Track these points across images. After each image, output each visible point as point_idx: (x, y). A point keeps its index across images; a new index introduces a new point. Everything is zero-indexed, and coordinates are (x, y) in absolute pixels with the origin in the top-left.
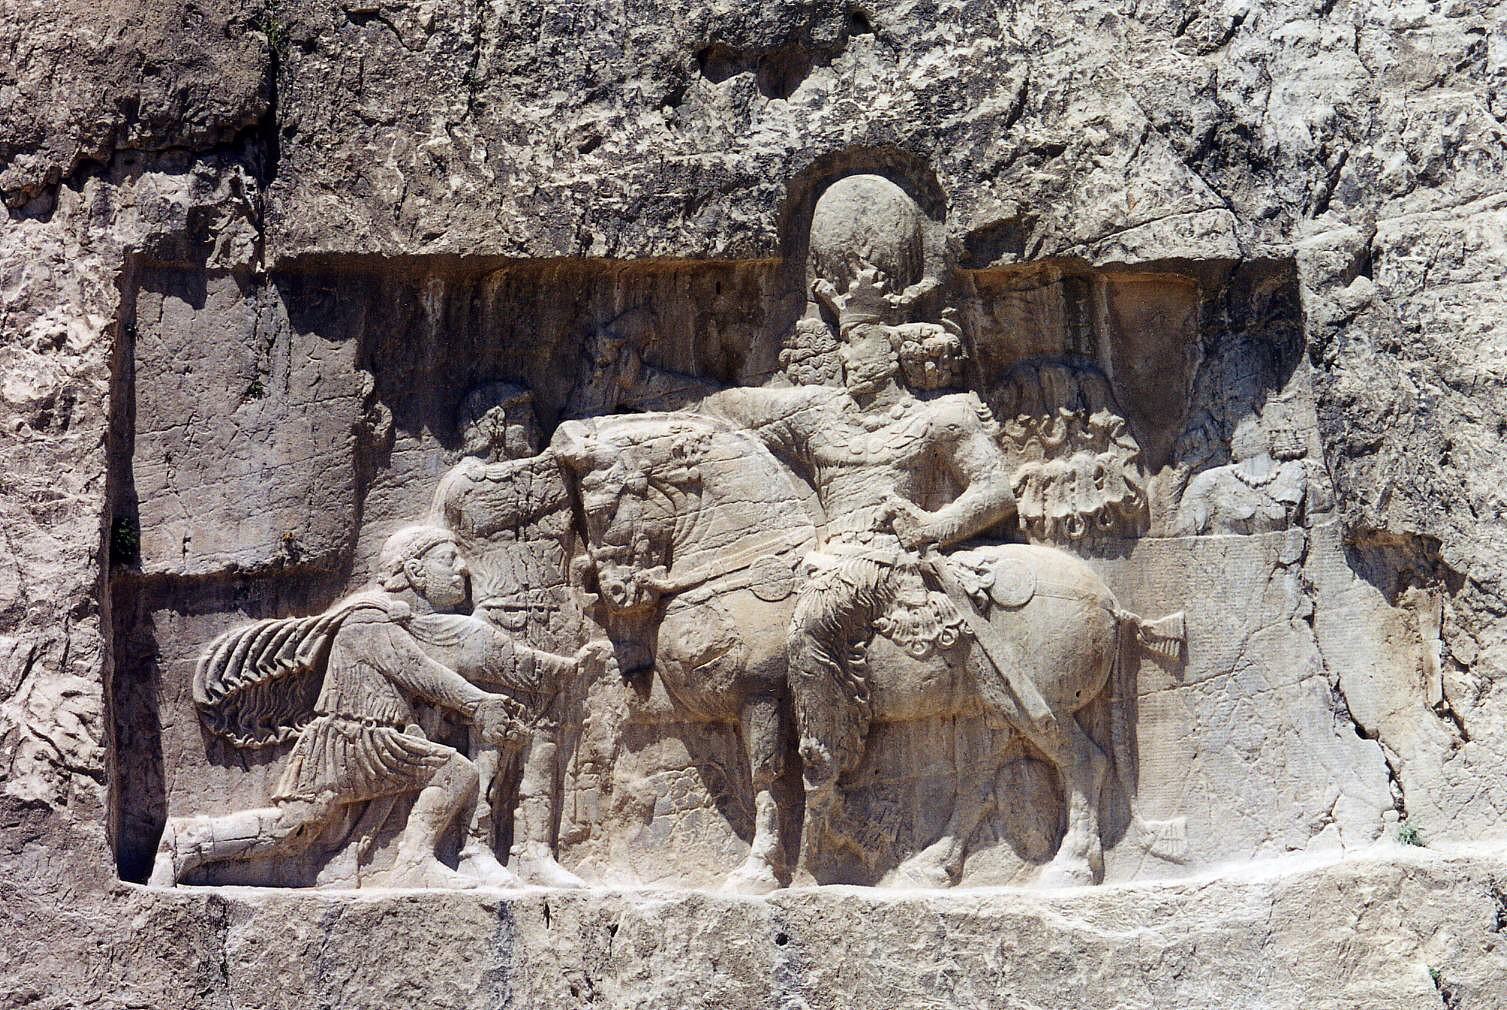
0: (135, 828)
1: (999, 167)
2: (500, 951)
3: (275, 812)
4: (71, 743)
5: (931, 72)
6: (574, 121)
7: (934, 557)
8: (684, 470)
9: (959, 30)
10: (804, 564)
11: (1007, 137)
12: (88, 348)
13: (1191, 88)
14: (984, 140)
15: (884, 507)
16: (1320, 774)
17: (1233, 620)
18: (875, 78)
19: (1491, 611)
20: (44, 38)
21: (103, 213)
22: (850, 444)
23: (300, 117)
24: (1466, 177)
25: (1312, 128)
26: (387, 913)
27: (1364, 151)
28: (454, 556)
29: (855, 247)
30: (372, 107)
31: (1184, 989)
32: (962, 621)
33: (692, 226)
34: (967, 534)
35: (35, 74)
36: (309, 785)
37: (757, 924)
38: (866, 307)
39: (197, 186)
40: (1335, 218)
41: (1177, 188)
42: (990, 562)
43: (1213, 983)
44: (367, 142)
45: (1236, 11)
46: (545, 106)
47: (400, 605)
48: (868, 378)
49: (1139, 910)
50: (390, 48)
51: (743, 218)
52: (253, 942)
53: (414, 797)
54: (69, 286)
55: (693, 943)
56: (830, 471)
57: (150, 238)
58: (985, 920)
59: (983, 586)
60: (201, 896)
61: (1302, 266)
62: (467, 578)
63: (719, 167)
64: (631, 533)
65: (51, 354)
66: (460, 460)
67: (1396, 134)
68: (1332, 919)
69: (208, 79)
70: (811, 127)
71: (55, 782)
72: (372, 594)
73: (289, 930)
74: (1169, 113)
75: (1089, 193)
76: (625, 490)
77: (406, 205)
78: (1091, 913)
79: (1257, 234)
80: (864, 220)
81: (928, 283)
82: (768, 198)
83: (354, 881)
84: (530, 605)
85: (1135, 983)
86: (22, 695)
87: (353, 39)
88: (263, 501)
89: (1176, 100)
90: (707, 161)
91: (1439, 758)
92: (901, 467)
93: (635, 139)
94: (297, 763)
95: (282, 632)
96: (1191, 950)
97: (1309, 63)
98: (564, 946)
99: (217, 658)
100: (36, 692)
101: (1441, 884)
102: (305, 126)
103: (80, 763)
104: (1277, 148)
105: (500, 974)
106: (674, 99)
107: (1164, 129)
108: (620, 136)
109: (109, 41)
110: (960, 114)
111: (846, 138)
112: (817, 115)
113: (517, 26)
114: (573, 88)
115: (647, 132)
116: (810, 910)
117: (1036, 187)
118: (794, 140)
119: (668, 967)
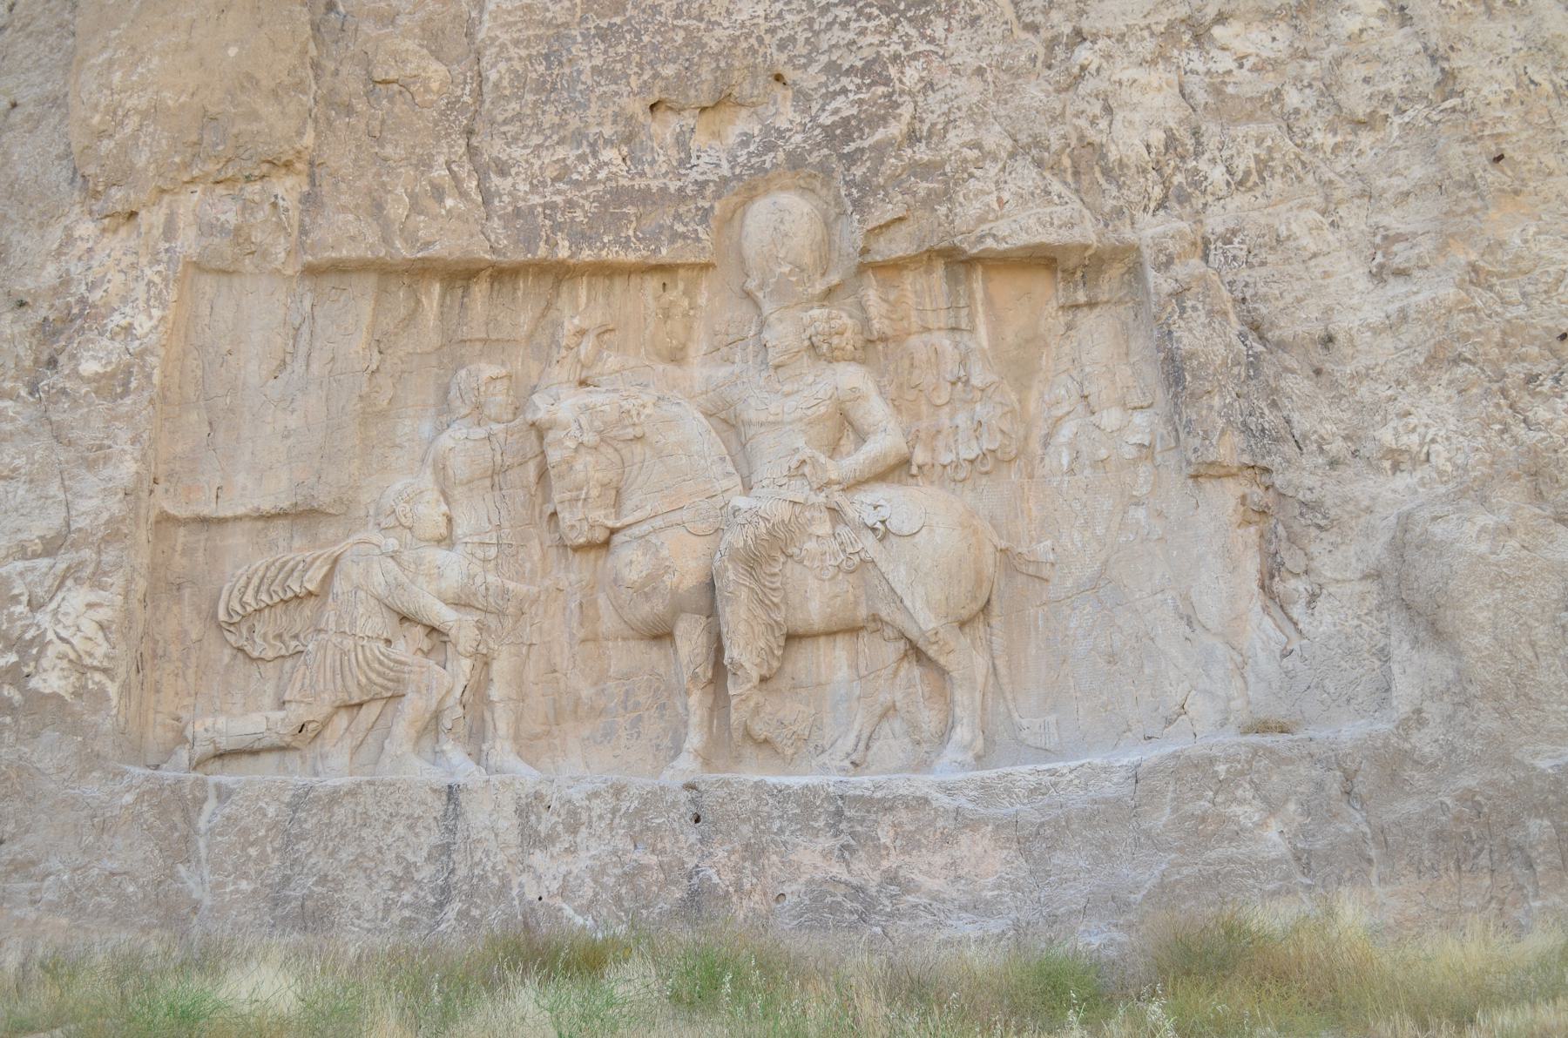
1: (896, 179)
2: (447, 828)
3: (281, 714)
4: (89, 646)
5: (836, 111)
7: (838, 497)
8: (630, 430)
9: (859, 81)
12: (147, 335)
15: (798, 457)
19: (1319, 527)
20: (136, 102)
21: (170, 231)
24: (1276, 184)
25: (1148, 147)
26: (347, 794)
27: (1191, 164)
30: (389, 150)
31: (1058, 858)
35: (128, 130)
39: (244, 208)
45: (1081, 60)
46: (525, 147)
47: (392, 543)
50: (405, 107)
51: (685, 229)
52: (228, 818)
53: (398, 696)
54: (141, 287)
55: (617, 820)
56: (751, 431)
58: (879, 800)
61: (1143, 248)
62: (450, 520)
63: (664, 190)
66: (448, 426)
67: (1216, 153)
68: (1190, 795)
69: (255, 127)
70: (739, 160)
71: (72, 679)
73: (261, 808)
75: (964, 195)
79: (1106, 225)
81: (834, 279)
85: (1012, 853)
86: (53, 605)
90: (655, 185)
91: (1278, 655)
93: (594, 171)
95: (292, 563)
98: (503, 824)
99: (238, 586)
100: (65, 603)
101: (1290, 761)
103: (96, 663)
104: (1121, 160)
105: (446, 849)
109: (182, 100)
110: (859, 141)
111: (768, 165)
114: (548, 132)
115: (606, 164)
116: (722, 793)
117: (922, 193)
118: (725, 170)
119: (593, 843)
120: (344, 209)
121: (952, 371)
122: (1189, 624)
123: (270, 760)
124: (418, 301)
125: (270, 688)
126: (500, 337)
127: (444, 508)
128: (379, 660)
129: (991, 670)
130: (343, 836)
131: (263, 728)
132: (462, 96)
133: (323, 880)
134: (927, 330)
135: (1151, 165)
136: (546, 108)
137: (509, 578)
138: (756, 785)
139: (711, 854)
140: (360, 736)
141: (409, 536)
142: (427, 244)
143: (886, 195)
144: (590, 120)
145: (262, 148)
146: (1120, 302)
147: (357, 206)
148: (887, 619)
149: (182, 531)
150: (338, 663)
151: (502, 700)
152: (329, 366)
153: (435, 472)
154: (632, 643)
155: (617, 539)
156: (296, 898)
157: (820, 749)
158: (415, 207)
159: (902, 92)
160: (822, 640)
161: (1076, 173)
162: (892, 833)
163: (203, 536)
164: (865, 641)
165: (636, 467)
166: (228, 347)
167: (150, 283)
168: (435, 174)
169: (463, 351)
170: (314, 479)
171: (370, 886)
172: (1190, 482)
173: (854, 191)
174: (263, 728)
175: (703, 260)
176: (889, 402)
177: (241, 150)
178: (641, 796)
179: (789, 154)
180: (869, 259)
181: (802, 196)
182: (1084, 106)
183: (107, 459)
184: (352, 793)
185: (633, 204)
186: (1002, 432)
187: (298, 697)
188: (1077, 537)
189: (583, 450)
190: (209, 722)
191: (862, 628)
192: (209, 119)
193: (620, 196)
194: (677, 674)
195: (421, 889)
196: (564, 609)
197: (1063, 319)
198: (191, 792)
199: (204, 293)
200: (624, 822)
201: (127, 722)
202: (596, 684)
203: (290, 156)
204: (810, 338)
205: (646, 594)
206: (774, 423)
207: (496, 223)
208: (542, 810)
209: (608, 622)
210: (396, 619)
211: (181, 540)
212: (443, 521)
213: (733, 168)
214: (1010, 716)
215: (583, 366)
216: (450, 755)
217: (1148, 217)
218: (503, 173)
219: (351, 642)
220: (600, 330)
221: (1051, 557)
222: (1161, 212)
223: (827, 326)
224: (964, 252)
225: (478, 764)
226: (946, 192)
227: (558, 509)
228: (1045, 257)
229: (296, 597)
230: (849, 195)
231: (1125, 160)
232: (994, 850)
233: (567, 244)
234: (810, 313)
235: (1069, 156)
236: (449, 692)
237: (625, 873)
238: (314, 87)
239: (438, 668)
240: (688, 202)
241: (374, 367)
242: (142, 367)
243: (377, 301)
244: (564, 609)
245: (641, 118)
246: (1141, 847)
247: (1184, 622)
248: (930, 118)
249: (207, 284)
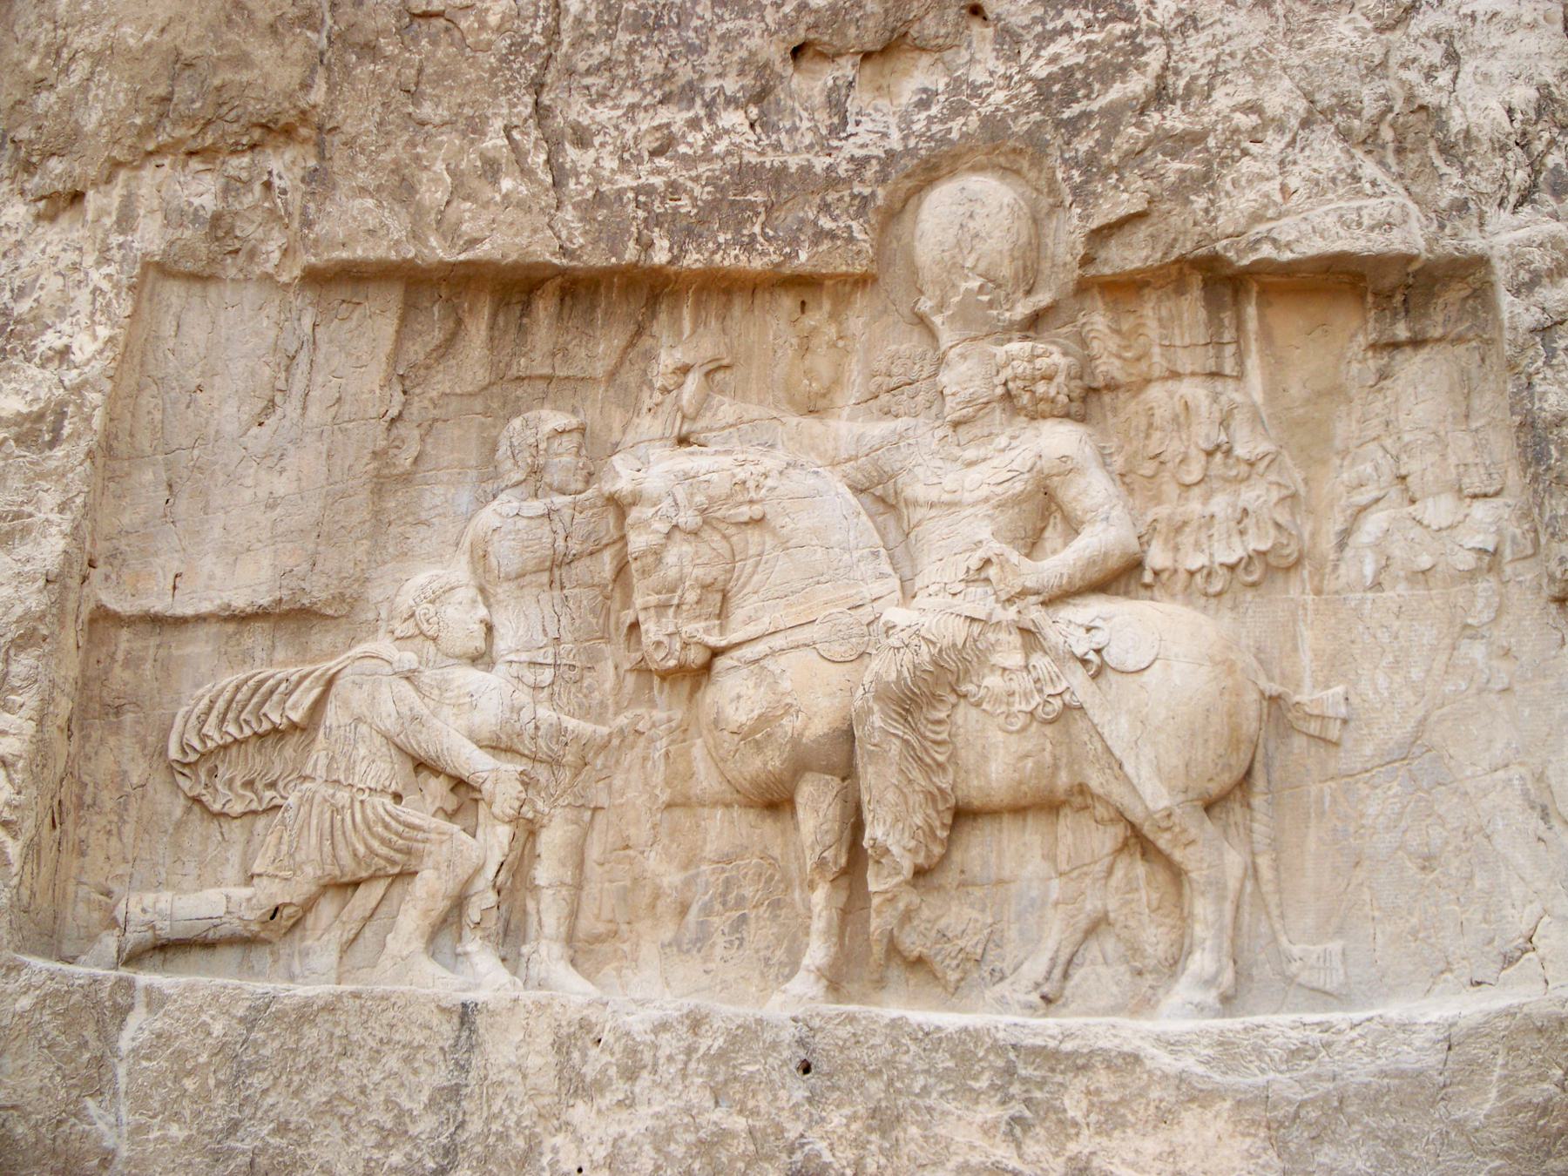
0: (89, 901)
2: (457, 1063)
3: (247, 892)
5: (1054, 59)
7: (1035, 614)
8: (745, 508)
9: (1088, 15)
10: (882, 620)
11: (1139, 125)
12: (89, 360)
13: (1362, 66)
14: (1112, 129)
15: (981, 554)
16: (1516, 890)
18: (992, 74)
20: (87, 41)
21: (126, 221)
23: (345, 120)
25: (1510, 111)
26: (323, 1009)
28: (474, 601)
30: (426, 110)
31: (1326, 1155)
33: (771, 233)
34: (1078, 583)
35: (75, 79)
36: (286, 863)
37: (775, 1046)
39: (226, 190)
40: (1538, 211)
41: (1343, 176)
43: (1363, 1150)
46: (615, 107)
49: (1271, 1050)
52: (159, 1036)
53: (407, 875)
54: (83, 296)
55: (692, 1065)
56: (918, 514)
57: (171, 244)
58: (1068, 1055)
60: (106, 978)
62: (490, 629)
63: (807, 170)
64: (681, 579)
65: (52, 366)
66: (495, 497)
68: (1528, 1072)
69: (245, 76)
72: (382, 645)
73: (204, 1023)
74: (1334, 95)
76: (676, 526)
77: (450, 210)
78: (1206, 1052)
79: (1442, 227)
80: (971, 224)
81: (1043, 298)
83: (333, 975)
85: (1259, 1143)
87: (415, 40)
88: (265, 535)
89: (1344, 80)
90: (794, 163)
92: (1001, 505)
93: (710, 141)
94: (276, 835)
95: (271, 682)
96: (1336, 1104)
97: (1506, 41)
98: (534, 1062)
102: (349, 129)
104: (1468, 131)
105: (454, 1092)
106: (760, 96)
107: (1328, 114)
108: (698, 138)
109: (147, 38)
110: (1085, 102)
111: (955, 135)
112: (923, 115)
113: (590, 24)
114: (648, 87)
115: (727, 132)
117: (1172, 178)
118: (895, 142)
119: (657, 1094)
120: (363, 191)
121: (1208, 436)
122: (1545, 816)
123: (230, 956)
125: (235, 855)
126: (571, 373)
127: (482, 612)
128: (383, 820)
129: (1250, 872)
130: (313, 1067)
131: (221, 911)
132: (530, 35)
133: (282, 1128)
134: (1175, 375)
135: (1513, 137)
136: (647, 52)
137: (568, 714)
138: (894, 1024)
139: (823, 1119)
140: (355, 927)
141: (432, 649)
142: (473, 242)
144: (707, 69)
145: (253, 106)
146: (1459, 339)
147: (379, 188)
148: (1100, 791)
149: (125, 634)
150: (327, 824)
151: (550, 886)
152: (333, 411)
153: (472, 561)
154: (736, 812)
155: (721, 663)
156: (244, 1153)
157: (997, 975)
158: (459, 189)
159: (1151, 32)
160: (1006, 818)
161: (1400, 151)
162: (1084, 1104)
163: (153, 641)
164: (1066, 824)
165: (751, 562)
166: (198, 381)
167: (97, 291)
168: (488, 144)
169: (519, 393)
170: (306, 566)
171: (347, 1140)
172: (1553, 607)
173: (1075, 173)
174: (221, 911)
175: (858, 269)
176: (1118, 478)
177: (225, 109)
178: (729, 1031)
179: (985, 121)
180: (1092, 271)
181: (1002, 178)
182: (1416, 51)
183: (26, 531)
184: (330, 1008)
185: (760, 189)
186: (1278, 526)
187: (271, 870)
188: (1382, 681)
189: (678, 536)
190: (149, 898)
191: (1064, 803)
192: (181, 65)
193: (745, 175)
194: (798, 858)
195: (419, 1149)
196: (645, 759)
197: (1373, 363)
198: (112, 994)
199: (169, 306)
200: (703, 1067)
201: (33, 894)
202: (685, 867)
203: (291, 116)
204: (1005, 384)
205: (757, 742)
206: (950, 504)
207: (569, 213)
208: (590, 1044)
209: (706, 780)
210: (410, 766)
211: (123, 646)
212: (480, 630)
213: (905, 138)
214: (1275, 939)
215: (684, 417)
216: (476, 959)
217: (1505, 215)
219: (347, 795)
220: (711, 366)
221: (1343, 710)
222: (1527, 209)
223: (1029, 367)
224: (1230, 263)
225: (515, 973)
226: (1206, 176)
227: (641, 619)
228: (1348, 273)
229: (275, 730)
230: (1070, 178)
231: (1474, 131)
232: (1232, 1136)
233: (666, 244)
234: (1008, 347)
235: (1392, 126)
236: (479, 870)
237: (701, 1141)
238: (329, 22)
239: (464, 836)
240: (840, 187)
241: (394, 412)
242: (80, 407)
243: (403, 320)
244: (645, 759)
245: (778, 67)
246: (1451, 1145)
247: (1536, 814)
248: (1189, 69)
249: (174, 293)
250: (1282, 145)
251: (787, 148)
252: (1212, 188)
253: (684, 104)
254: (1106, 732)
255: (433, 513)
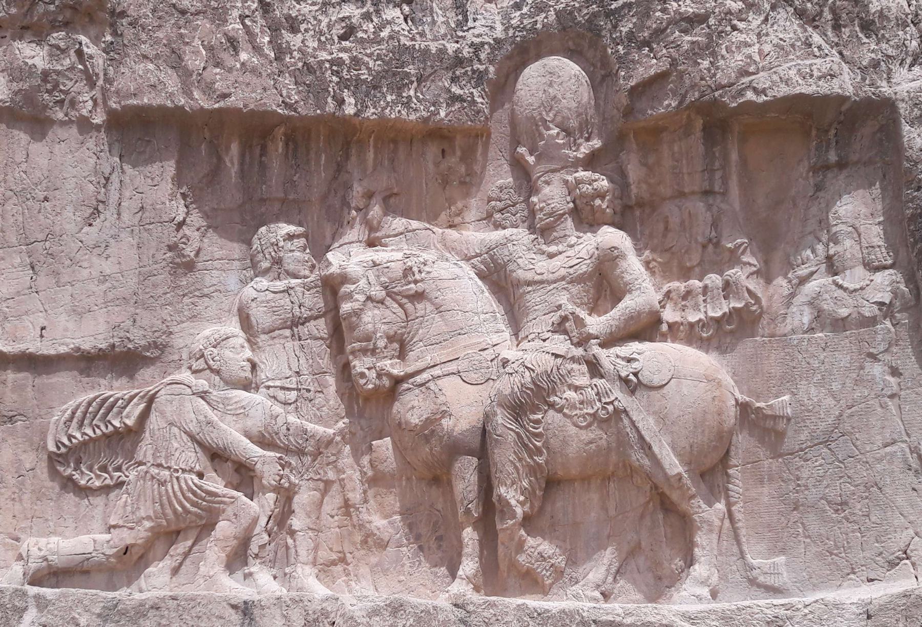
6: (335, 14)
7: (596, 350)
8: (412, 285)
15: (561, 313)
17: (830, 401)
22: (536, 268)
29: (544, 113)
32: (617, 398)
33: (421, 97)
38: (551, 159)
42: (639, 354)
44: (180, 28)
46: (314, 4)
48: (550, 215)
51: (461, 92)
59: (632, 370)
62: (254, 366)
63: (442, 51)
70: (513, 22)
76: (369, 298)
80: (551, 90)
82: (479, 78)
84: (300, 387)
90: (433, 47)
115: (389, 23)
124: (220, 159)
143: (651, 50)
212: (248, 366)
213: (506, 30)
218: (294, 30)
236: (255, 521)
250: (759, 22)
251: (429, 37)
252: (714, 54)
253: (360, 4)
254: (640, 425)
255: (212, 289)
